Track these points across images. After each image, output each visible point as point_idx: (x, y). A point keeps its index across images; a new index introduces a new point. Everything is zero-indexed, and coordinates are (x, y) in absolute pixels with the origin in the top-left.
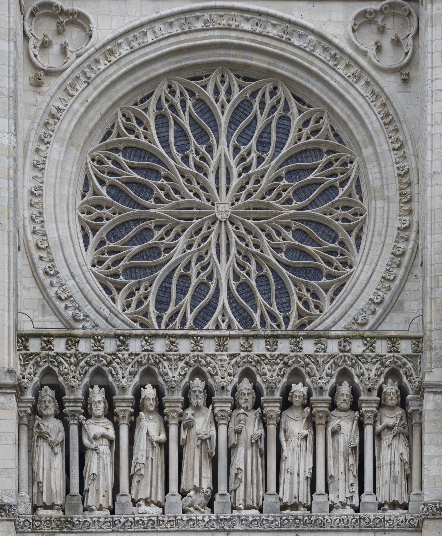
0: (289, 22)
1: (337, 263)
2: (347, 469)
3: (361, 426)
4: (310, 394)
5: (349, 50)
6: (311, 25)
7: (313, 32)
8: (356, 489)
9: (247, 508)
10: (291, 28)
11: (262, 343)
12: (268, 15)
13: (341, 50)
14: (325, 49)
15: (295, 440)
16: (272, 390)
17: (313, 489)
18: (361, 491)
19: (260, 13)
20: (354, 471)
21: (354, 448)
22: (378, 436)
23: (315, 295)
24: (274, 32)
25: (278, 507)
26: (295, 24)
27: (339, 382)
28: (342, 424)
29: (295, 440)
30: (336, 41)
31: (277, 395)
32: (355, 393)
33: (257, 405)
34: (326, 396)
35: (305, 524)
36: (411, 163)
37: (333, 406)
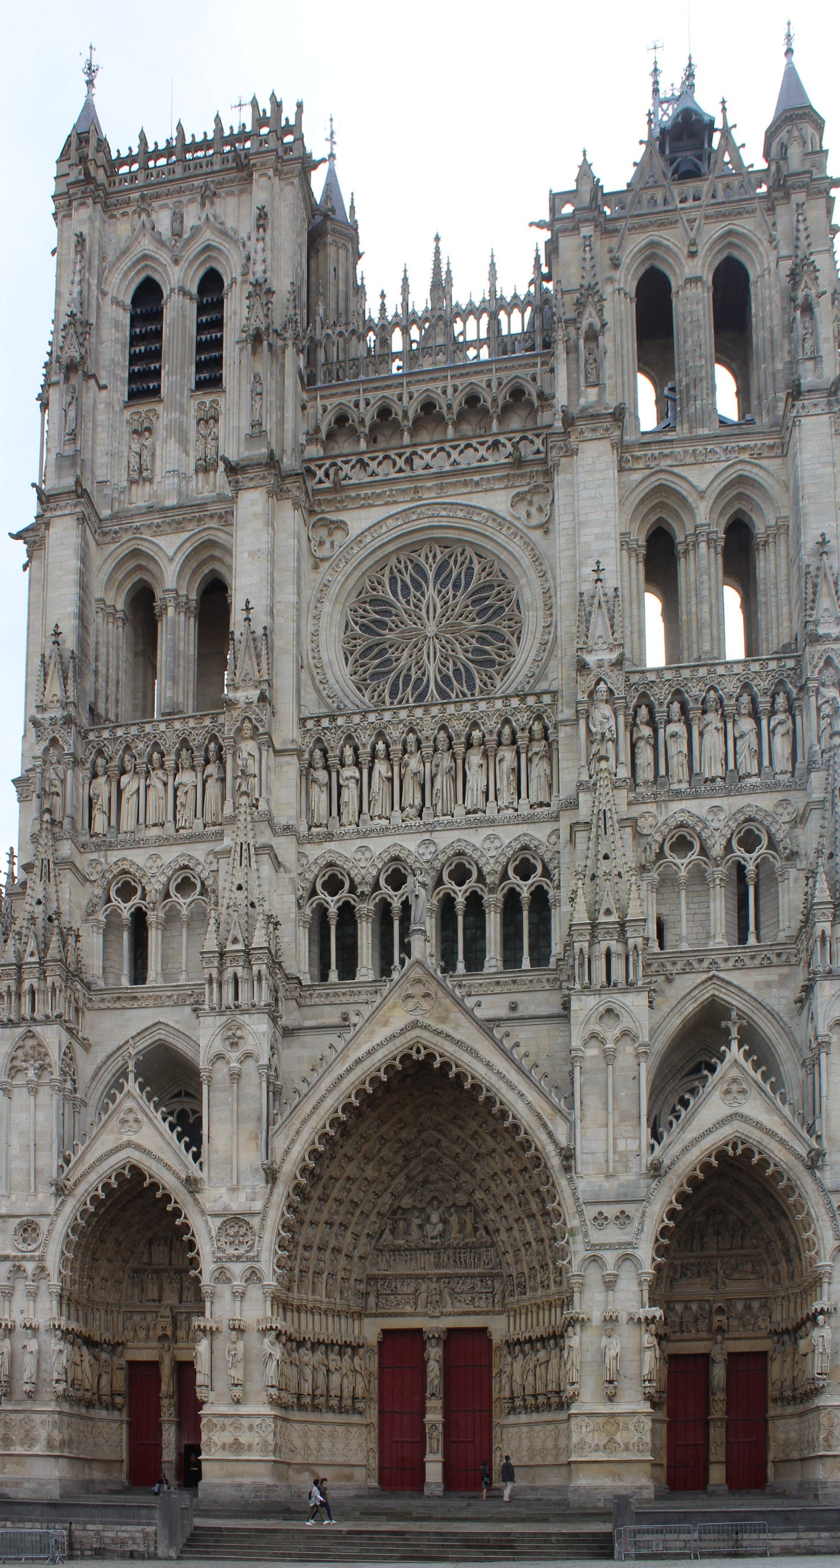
0: (471, 506)
1: (505, 655)
2: (509, 784)
3: (518, 754)
4: (484, 736)
5: (509, 518)
6: (484, 506)
7: (485, 510)
8: (515, 796)
9: (444, 815)
10: (471, 510)
11: (453, 706)
12: (457, 504)
13: (504, 519)
14: (494, 520)
15: (474, 767)
16: (458, 736)
17: (487, 799)
18: (519, 797)
19: (452, 504)
20: (514, 784)
21: (513, 769)
22: (529, 760)
23: (491, 678)
24: (460, 514)
25: (464, 812)
26: (474, 507)
27: (503, 727)
28: (506, 754)
29: (474, 767)
30: (500, 514)
31: (463, 740)
32: (514, 733)
33: (450, 747)
34: (495, 737)
35: (481, 822)
36: (551, 584)
37: (500, 743)
